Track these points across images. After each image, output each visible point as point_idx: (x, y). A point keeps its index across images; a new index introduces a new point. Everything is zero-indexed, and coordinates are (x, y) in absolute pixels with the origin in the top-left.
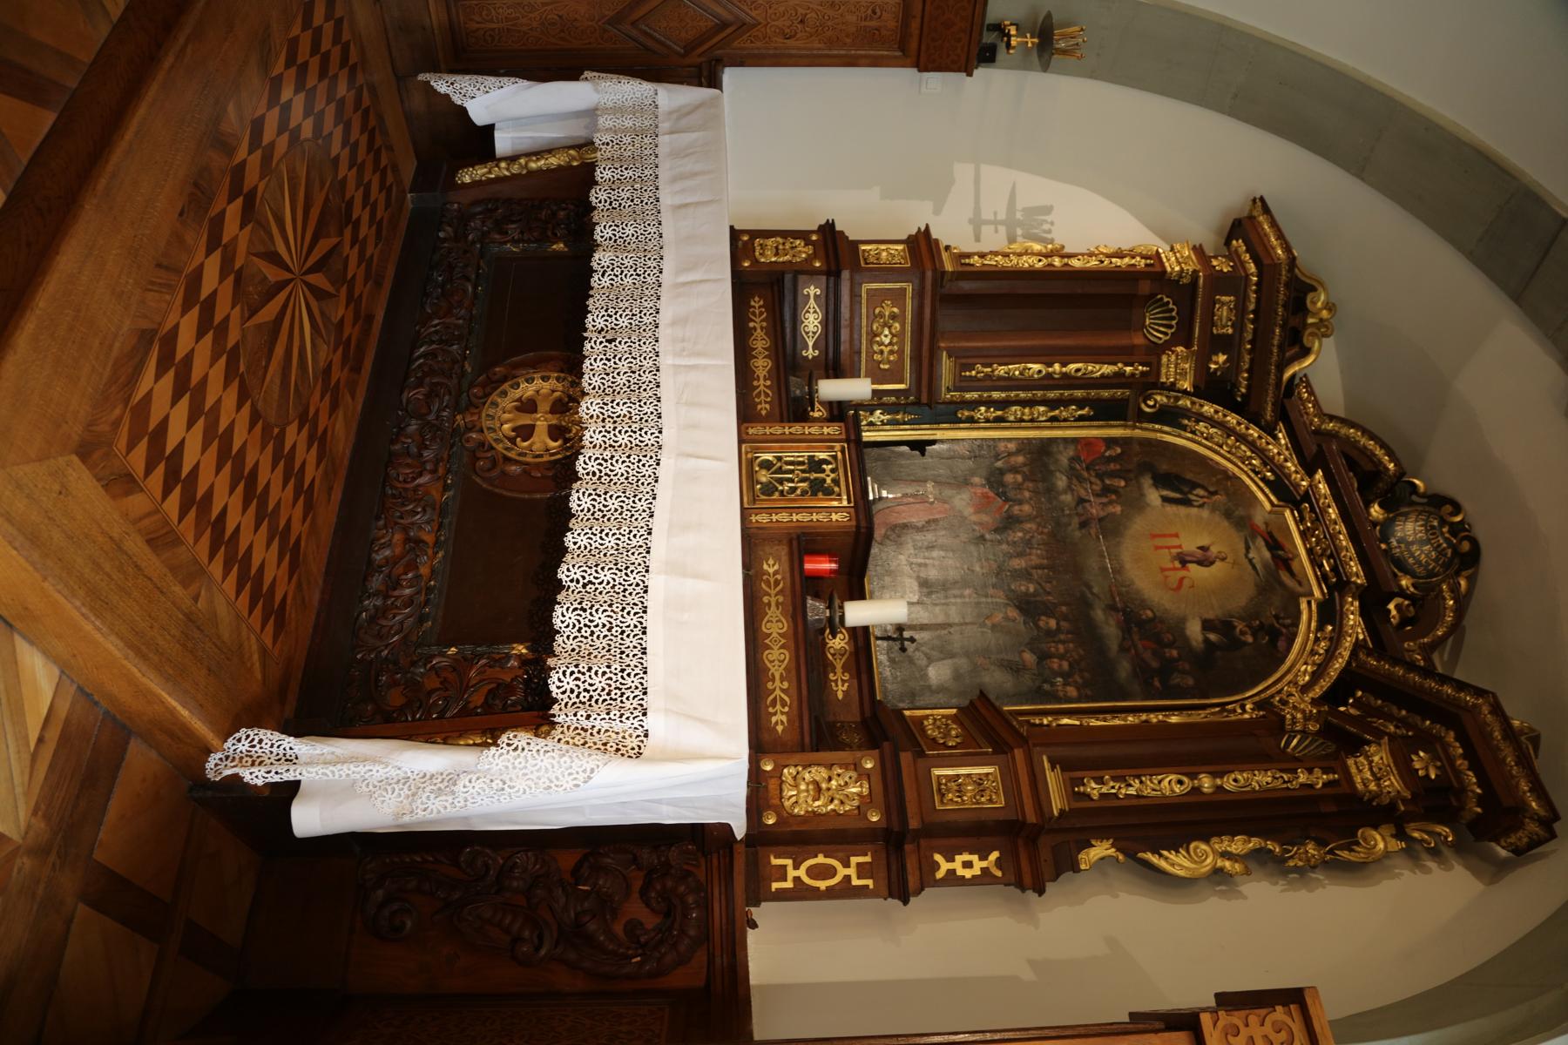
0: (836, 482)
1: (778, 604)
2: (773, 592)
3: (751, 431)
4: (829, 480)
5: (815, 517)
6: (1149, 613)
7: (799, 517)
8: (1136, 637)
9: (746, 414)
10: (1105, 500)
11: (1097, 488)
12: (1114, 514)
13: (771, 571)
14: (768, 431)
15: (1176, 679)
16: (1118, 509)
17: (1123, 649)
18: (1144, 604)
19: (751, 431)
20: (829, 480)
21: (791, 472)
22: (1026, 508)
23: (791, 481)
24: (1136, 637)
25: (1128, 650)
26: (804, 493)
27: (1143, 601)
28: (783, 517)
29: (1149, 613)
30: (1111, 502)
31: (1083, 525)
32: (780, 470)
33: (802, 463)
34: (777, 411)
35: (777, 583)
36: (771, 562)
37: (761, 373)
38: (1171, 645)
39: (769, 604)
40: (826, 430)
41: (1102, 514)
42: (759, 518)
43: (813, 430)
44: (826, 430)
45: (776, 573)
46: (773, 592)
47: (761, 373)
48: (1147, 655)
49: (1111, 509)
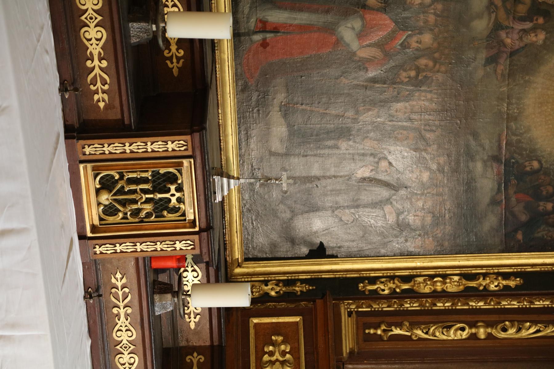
0: (179, 200)
1: (127, 315)
2: (121, 305)
3: (87, 150)
4: (174, 200)
5: (159, 246)
6: (536, 164)
7: (144, 247)
8: (511, 191)
9: (80, 127)
10: (528, 25)
11: (522, 9)
12: (532, 44)
13: (119, 284)
14: (107, 149)
15: (542, 232)
16: (542, 36)
17: (494, 202)
18: (533, 154)
19: (87, 150)
20: (174, 200)
21: (134, 192)
22: (427, 38)
23: (135, 202)
24: (511, 191)
25: (499, 203)
26: (149, 215)
27: (533, 151)
28: (126, 247)
29: (536, 164)
30: (534, 29)
31: (492, 60)
32: (121, 191)
33: (145, 181)
34: (117, 103)
35: (125, 297)
36: (119, 276)
37: (95, 49)
38: (548, 199)
39: (118, 315)
40: (170, 146)
41: (518, 45)
42: (103, 249)
43: (155, 147)
44: (170, 146)
45: (123, 287)
46: (121, 305)
47: (95, 49)
48: (518, 209)
49: (532, 38)
